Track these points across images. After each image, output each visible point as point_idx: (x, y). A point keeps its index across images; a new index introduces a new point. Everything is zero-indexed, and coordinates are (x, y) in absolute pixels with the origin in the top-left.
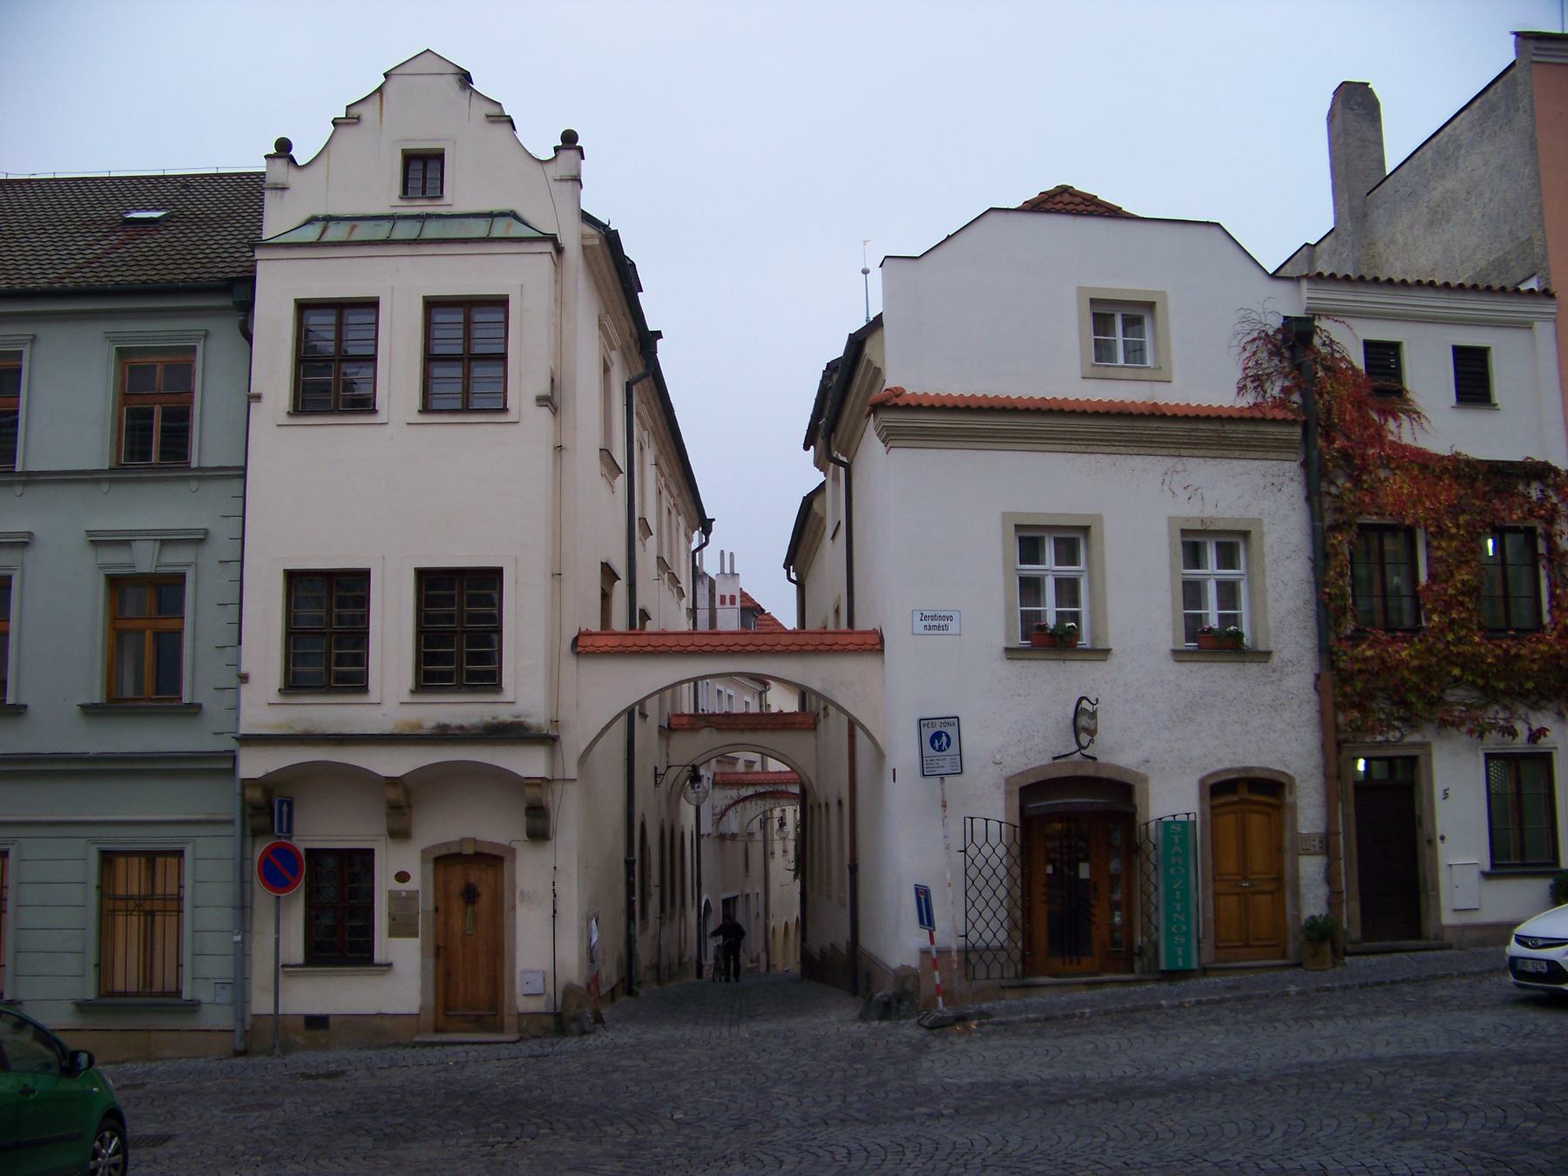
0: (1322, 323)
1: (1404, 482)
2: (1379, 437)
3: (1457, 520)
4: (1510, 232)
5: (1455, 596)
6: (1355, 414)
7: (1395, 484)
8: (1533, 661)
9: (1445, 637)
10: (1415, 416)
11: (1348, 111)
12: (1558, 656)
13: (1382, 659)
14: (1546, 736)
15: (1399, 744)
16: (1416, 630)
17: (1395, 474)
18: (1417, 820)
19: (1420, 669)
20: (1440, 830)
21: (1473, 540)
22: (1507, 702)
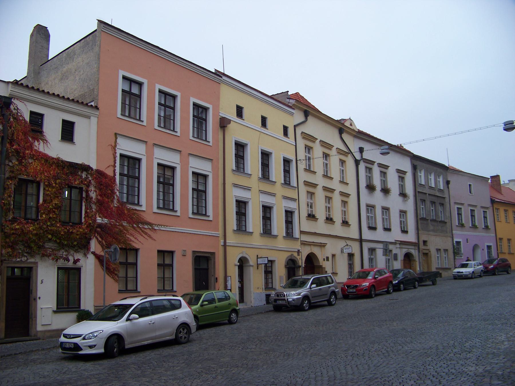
0: (15, 101)
1: (38, 165)
2: (31, 147)
3: (56, 182)
4: (87, 86)
5: (52, 209)
6: (23, 137)
7: (35, 165)
8: (77, 235)
9: (47, 223)
10: (45, 142)
11: (38, 35)
12: (86, 234)
13: (22, 229)
14: (79, 262)
15: (26, 262)
16: (37, 220)
17: (35, 161)
18: (30, 291)
19: (36, 235)
20: (39, 294)
21: (61, 189)
22: (67, 249)
